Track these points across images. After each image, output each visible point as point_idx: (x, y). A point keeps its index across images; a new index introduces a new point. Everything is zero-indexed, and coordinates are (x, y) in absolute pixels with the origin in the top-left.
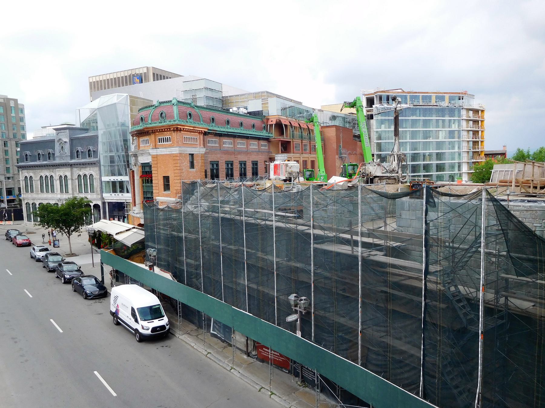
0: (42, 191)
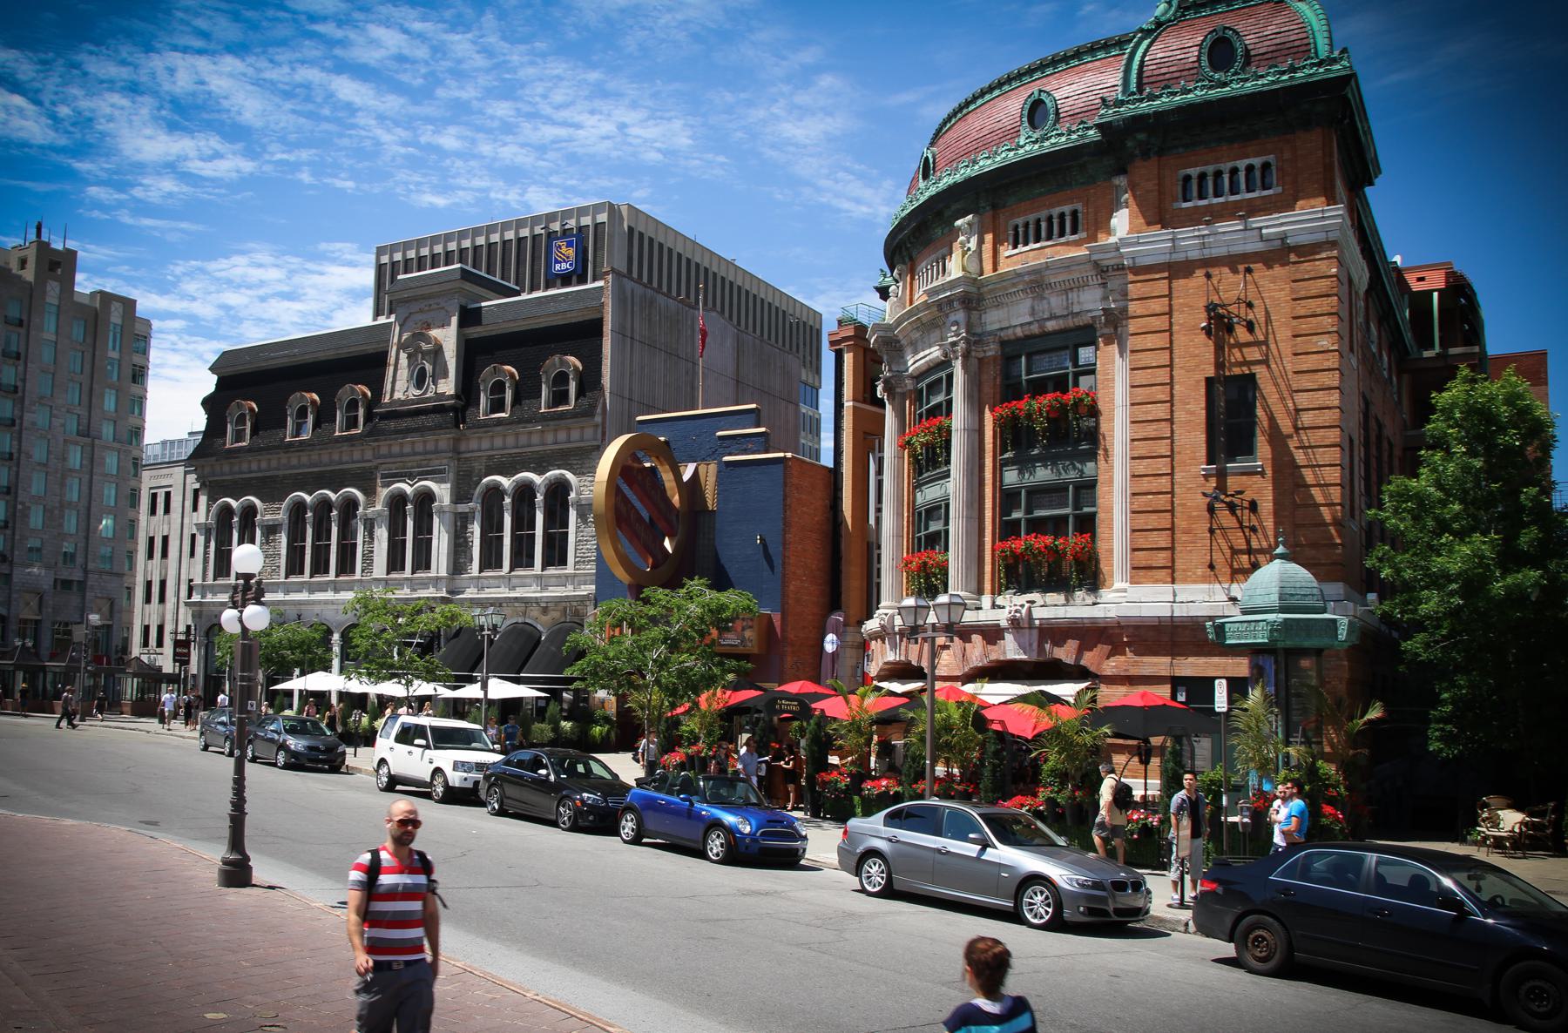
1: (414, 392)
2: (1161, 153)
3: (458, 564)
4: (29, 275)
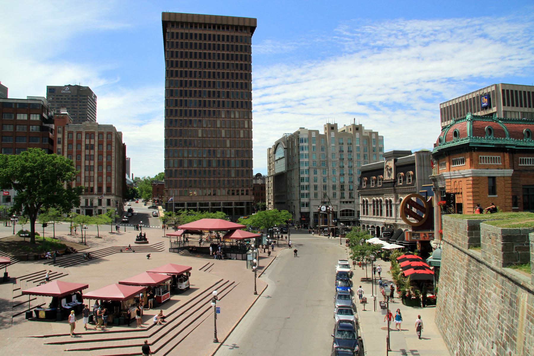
0: (374, 214)
1: (388, 178)
2: (449, 155)
3: (396, 216)
4: (352, 132)
